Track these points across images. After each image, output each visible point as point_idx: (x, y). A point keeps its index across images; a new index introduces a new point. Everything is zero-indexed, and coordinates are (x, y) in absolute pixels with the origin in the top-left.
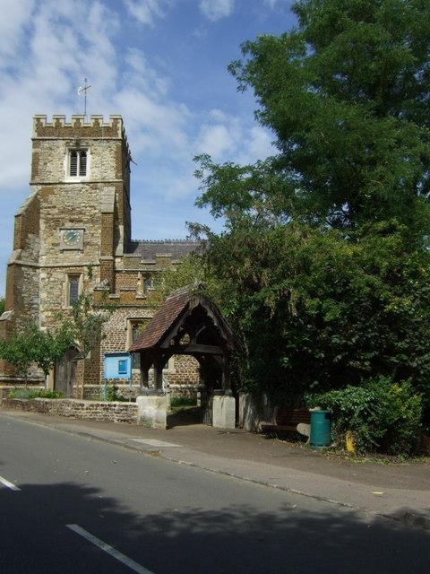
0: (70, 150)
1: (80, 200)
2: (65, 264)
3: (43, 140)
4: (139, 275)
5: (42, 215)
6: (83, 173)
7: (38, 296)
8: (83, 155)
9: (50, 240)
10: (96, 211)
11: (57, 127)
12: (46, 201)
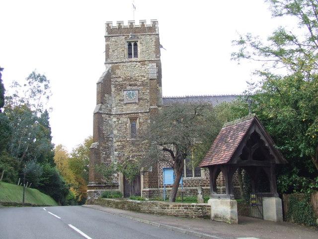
0: (127, 42)
1: (135, 72)
2: (128, 112)
6: (136, 55)
7: (112, 133)
8: (136, 45)
9: (118, 98)
10: (145, 79)
11: (119, 28)
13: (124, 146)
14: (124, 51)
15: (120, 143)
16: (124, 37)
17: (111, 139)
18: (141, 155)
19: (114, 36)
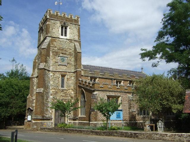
0: (61, 25)
2: (60, 71)
3: (51, 19)
4: (89, 78)
5: (51, 50)
6: (66, 35)
7: (49, 83)
8: (66, 28)
10: (72, 51)
11: (57, 15)
12: (52, 44)
13: (56, 93)
15: (54, 90)
17: (49, 87)
18: (67, 99)
19: (53, 20)
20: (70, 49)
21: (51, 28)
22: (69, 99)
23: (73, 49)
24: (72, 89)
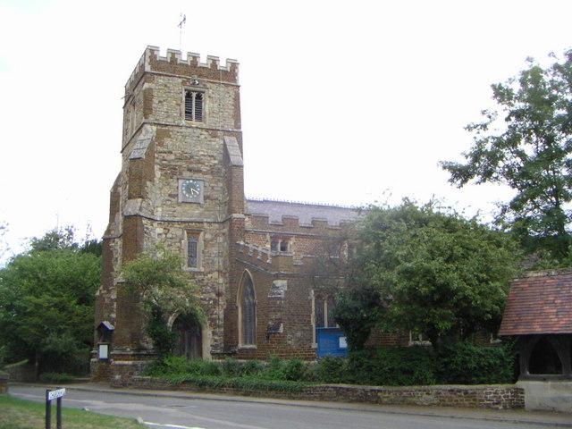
2: (184, 219)
3: (156, 74)
4: (268, 236)
6: (199, 117)
8: (199, 97)
9: (167, 190)
10: (216, 162)
12: (161, 144)
14: (179, 105)
16: (180, 80)
20: (212, 156)
21: (155, 101)
22: (210, 299)
23: (220, 157)
24: (219, 271)
